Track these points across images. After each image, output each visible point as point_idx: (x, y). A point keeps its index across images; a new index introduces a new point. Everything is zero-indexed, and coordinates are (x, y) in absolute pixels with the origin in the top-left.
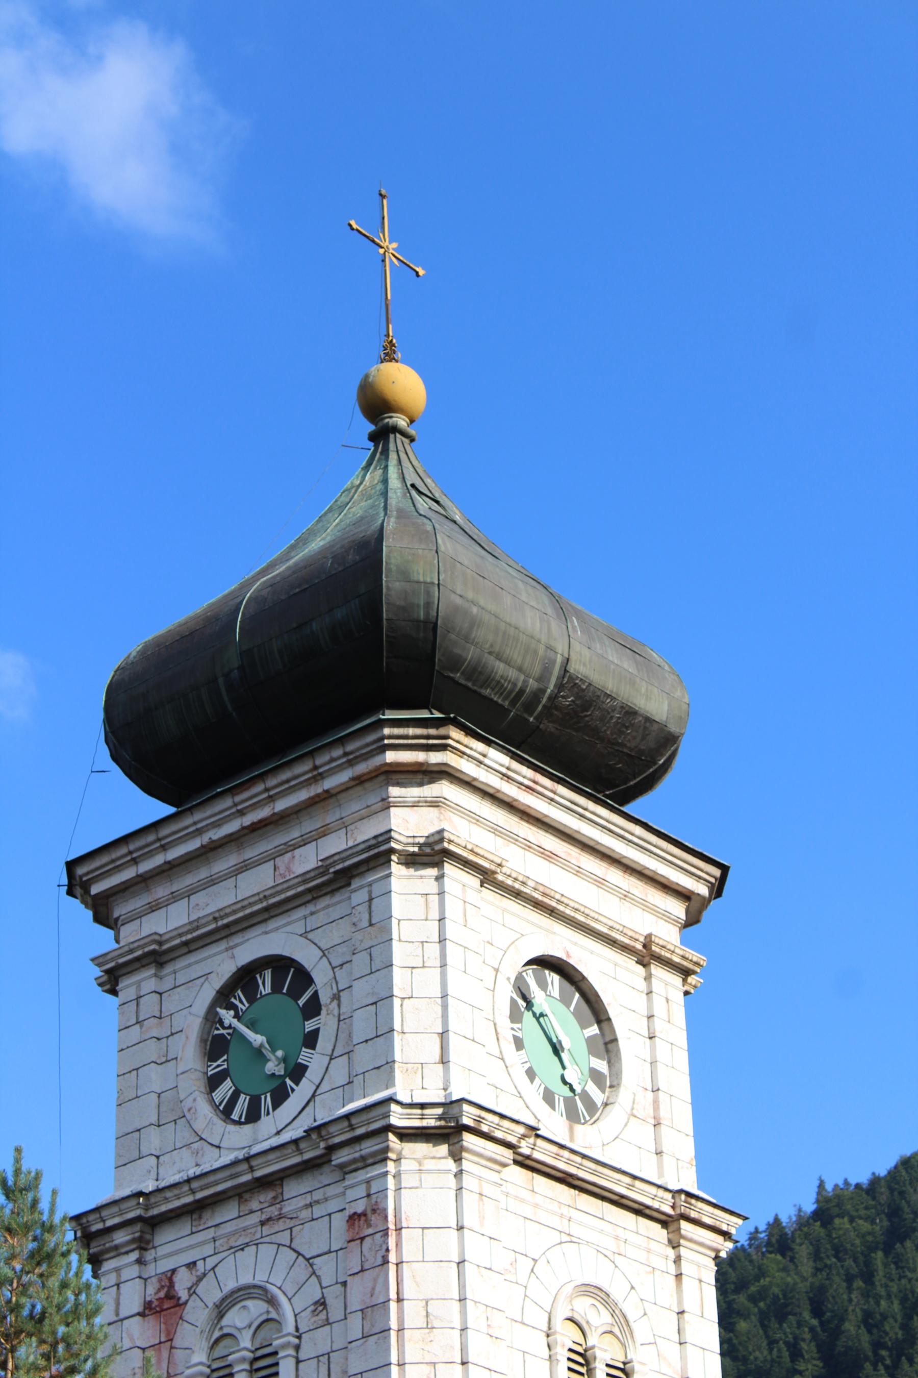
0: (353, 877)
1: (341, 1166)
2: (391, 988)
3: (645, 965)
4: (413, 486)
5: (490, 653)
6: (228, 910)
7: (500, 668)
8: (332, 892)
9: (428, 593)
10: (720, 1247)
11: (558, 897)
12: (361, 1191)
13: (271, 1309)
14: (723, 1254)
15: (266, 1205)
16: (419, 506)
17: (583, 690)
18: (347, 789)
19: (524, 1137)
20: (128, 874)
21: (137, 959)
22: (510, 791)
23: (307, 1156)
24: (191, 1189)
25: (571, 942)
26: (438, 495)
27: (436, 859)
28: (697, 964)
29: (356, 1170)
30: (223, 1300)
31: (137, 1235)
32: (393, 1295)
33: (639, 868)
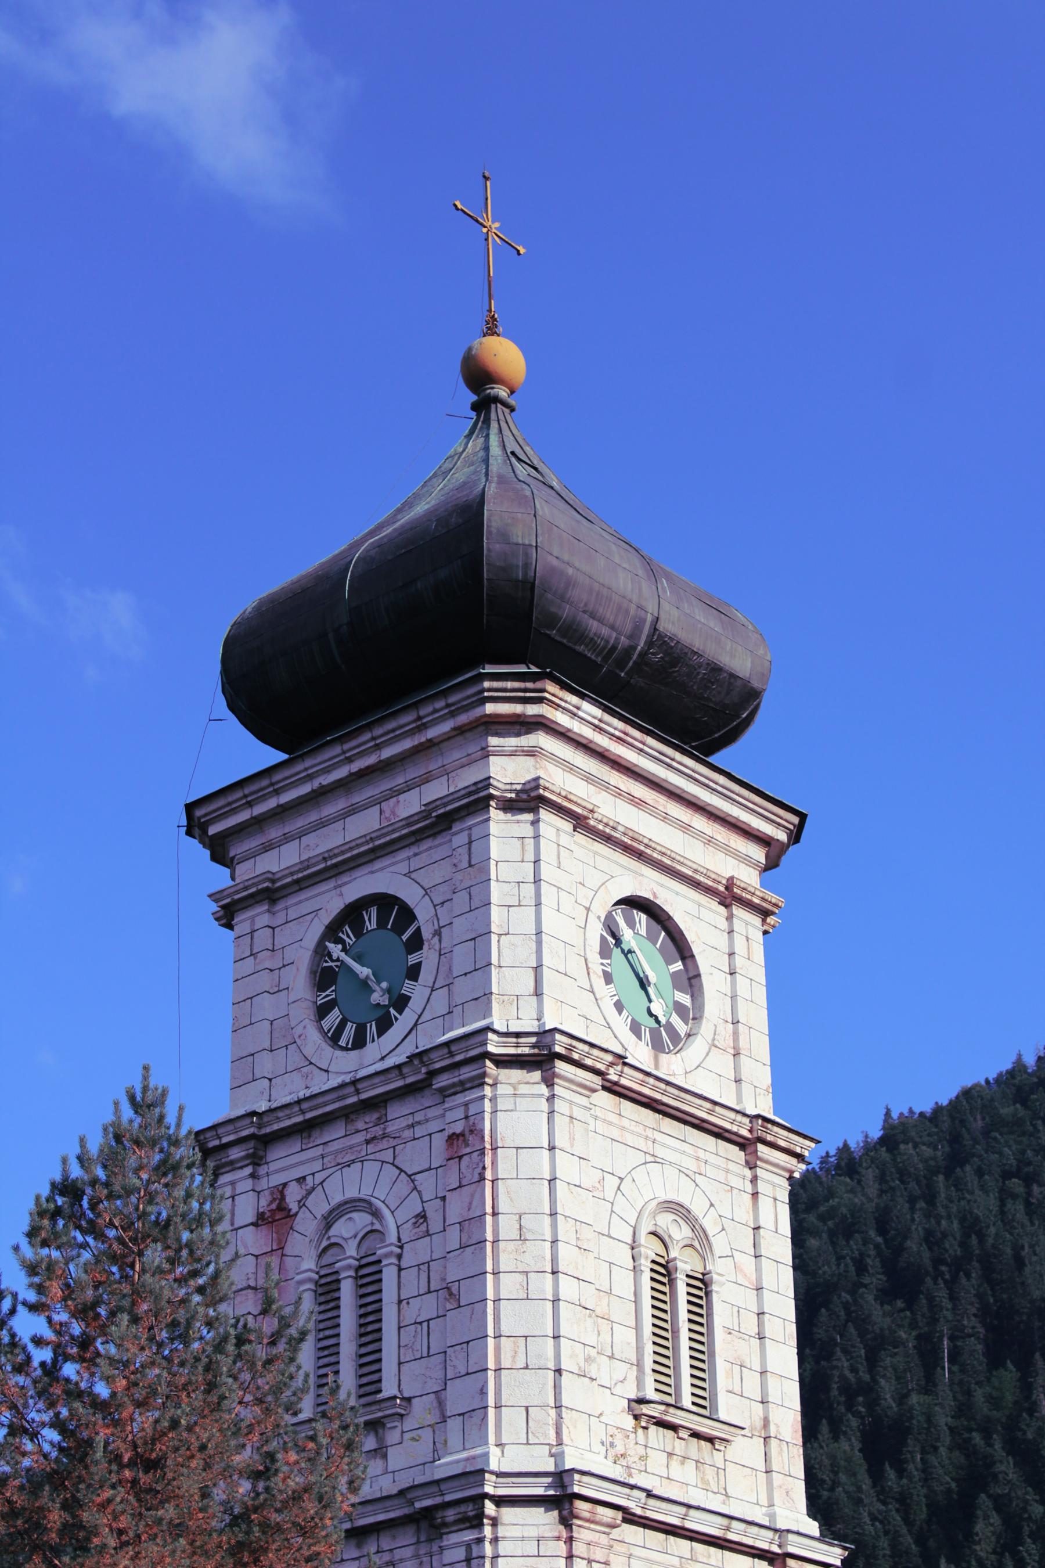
0: (454, 821)
1: (441, 1090)
2: (489, 925)
4: (513, 453)
5: (584, 612)
6: (336, 851)
7: (594, 626)
8: (434, 835)
9: (527, 555)
10: (794, 1168)
11: (646, 841)
12: (460, 1113)
13: (375, 1221)
14: (797, 1175)
15: (371, 1125)
16: (518, 472)
17: (672, 647)
18: (449, 738)
19: (612, 1064)
20: (244, 816)
21: (251, 896)
22: (602, 741)
23: (409, 1080)
24: (301, 1110)
25: (658, 883)
26: (536, 462)
27: (532, 804)
28: (776, 905)
29: (455, 1094)
30: (331, 1212)
31: (251, 1151)
32: (489, 1209)
33: (722, 815)
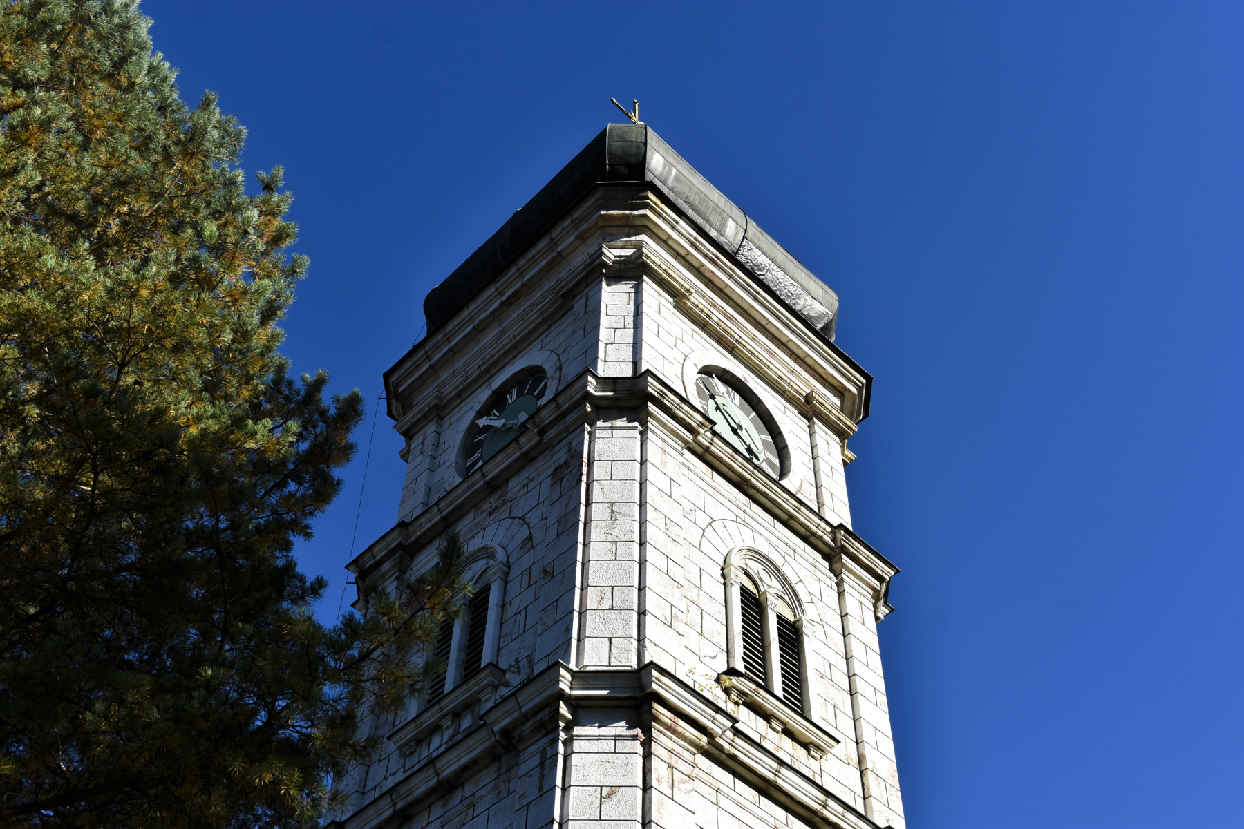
3: (809, 419)
